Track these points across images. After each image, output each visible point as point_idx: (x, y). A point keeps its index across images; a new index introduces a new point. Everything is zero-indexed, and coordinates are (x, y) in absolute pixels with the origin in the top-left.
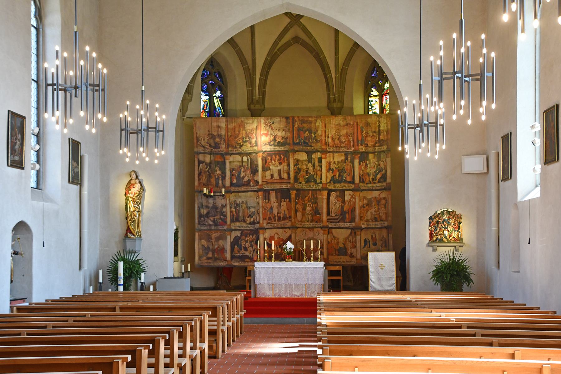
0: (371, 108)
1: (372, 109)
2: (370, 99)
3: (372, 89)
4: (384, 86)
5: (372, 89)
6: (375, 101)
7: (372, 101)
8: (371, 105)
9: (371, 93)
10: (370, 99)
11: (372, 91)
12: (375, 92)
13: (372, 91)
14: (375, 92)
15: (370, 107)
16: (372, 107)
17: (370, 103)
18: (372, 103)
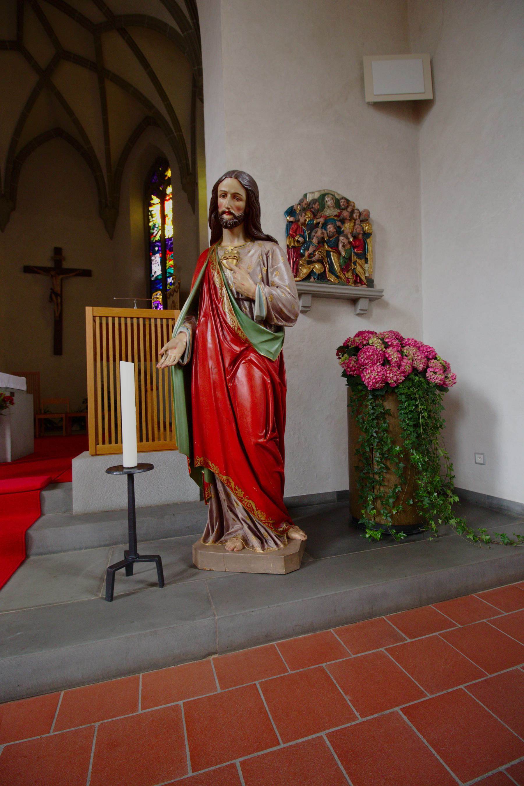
0: (151, 218)
1: (153, 219)
2: (151, 209)
3: (153, 197)
4: (166, 191)
5: (153, 197)
6: (156, 210)
7: (152, 211)
8: (152, 215)
9: (152, 202)
10: (151, 209)
11: (152, 199)
12: (155, 200)
13: (152, 199)
14: (155, 200)
15: (150, 217)
16: (152, 217)
17: (151, 213)
18: (153, 212)
